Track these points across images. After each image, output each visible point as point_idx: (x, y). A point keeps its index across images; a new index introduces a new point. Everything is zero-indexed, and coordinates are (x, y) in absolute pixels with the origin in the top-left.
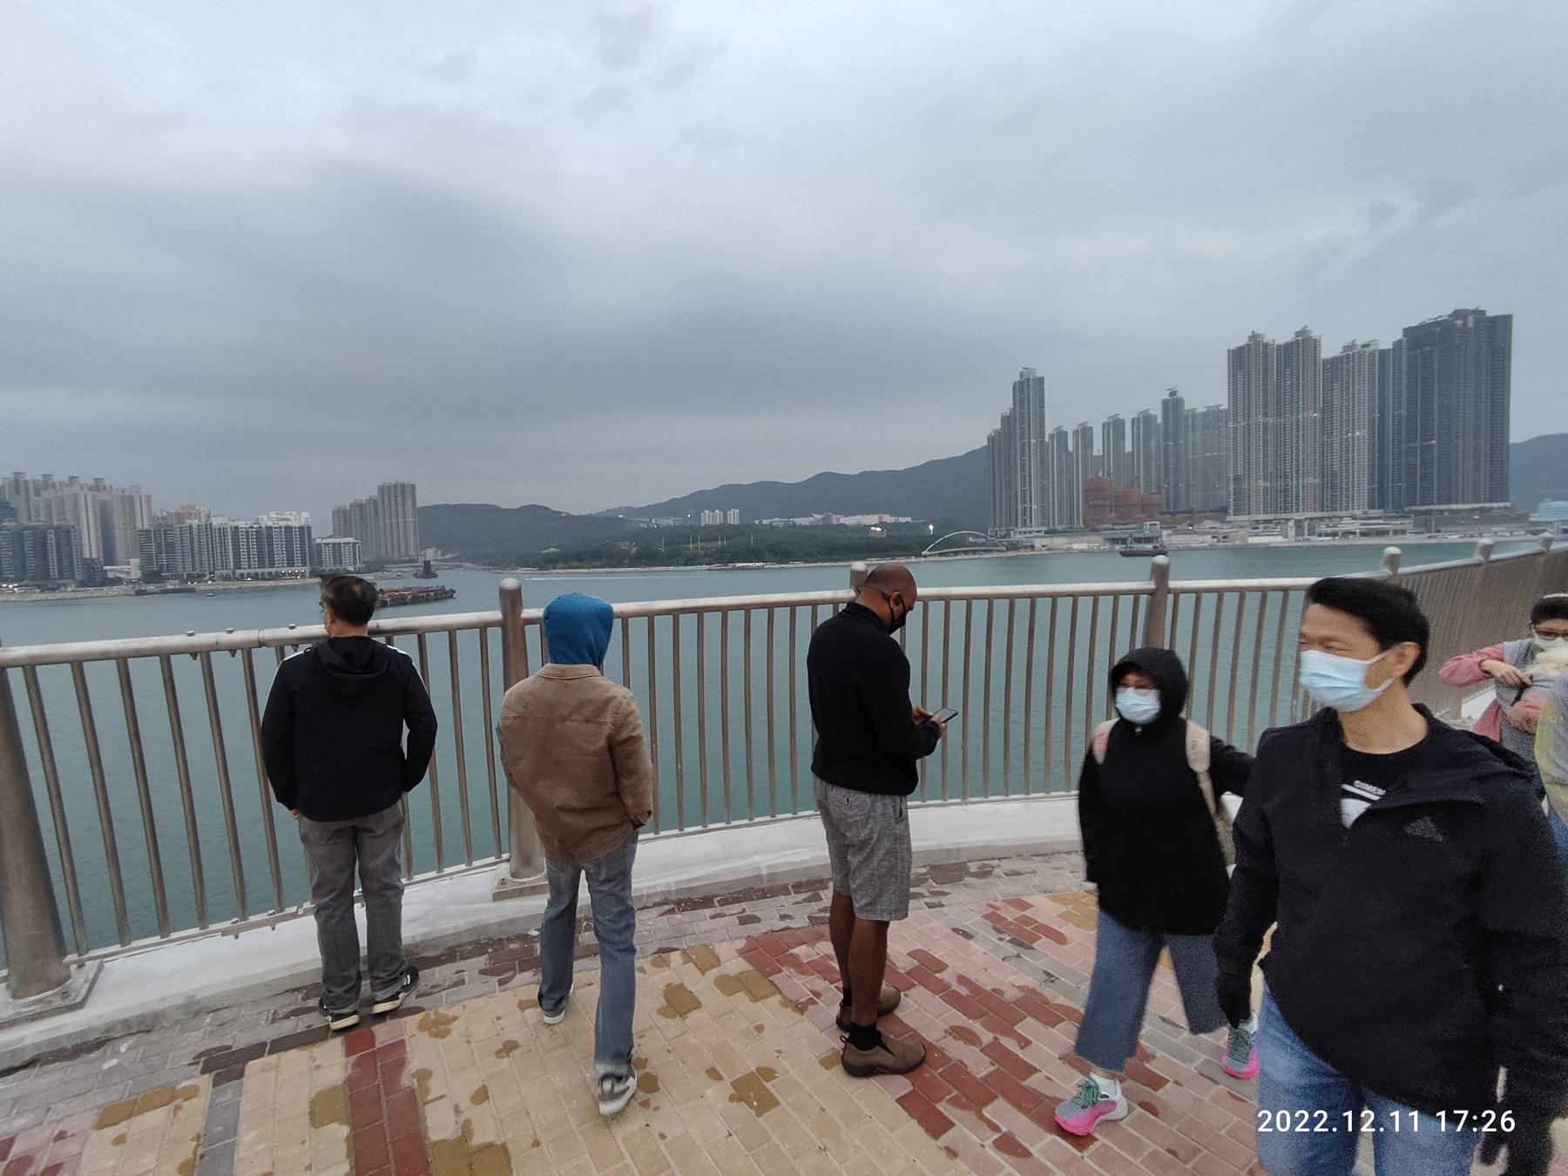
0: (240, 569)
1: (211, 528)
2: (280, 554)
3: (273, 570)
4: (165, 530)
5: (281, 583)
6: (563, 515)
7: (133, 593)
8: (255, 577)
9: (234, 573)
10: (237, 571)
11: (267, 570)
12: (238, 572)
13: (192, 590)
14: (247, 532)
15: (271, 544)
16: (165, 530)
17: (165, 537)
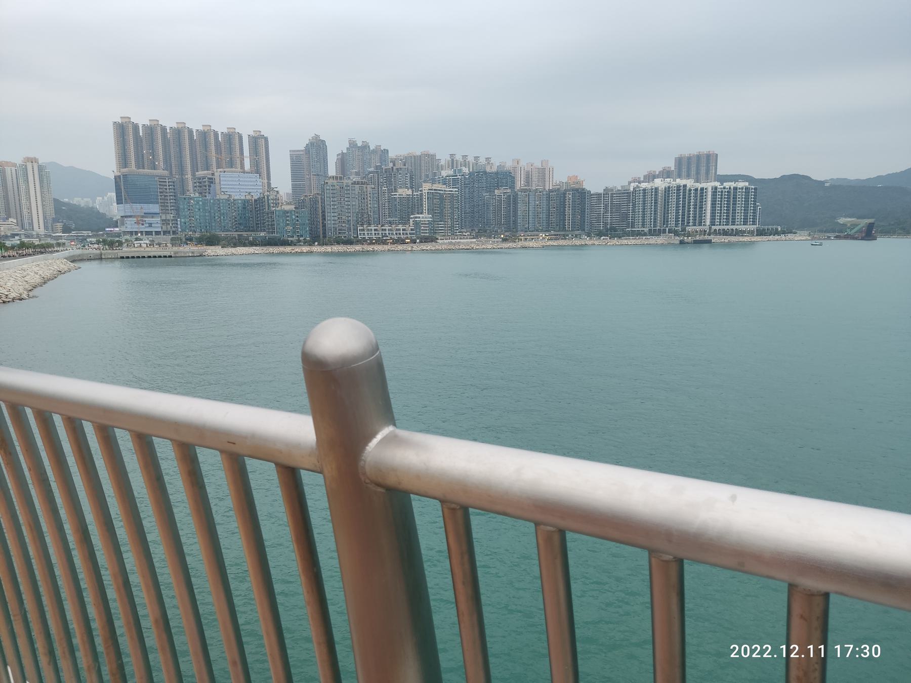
0: (714, 225)
1: (684, 192)
2: (739, 216)
3: (734, 227)
4: (612, 194)
5: (741, 239)
6: (827, 185)
7: (678, 242)
8: (725, 233)
9: (710, 228)
10: (713, 227)
11: (730, 227)
12: (714, 227)
13: (709, 242)
14: (722, 192)
15: (734, 204)
16: (612, 194)
17: (612, 199)
